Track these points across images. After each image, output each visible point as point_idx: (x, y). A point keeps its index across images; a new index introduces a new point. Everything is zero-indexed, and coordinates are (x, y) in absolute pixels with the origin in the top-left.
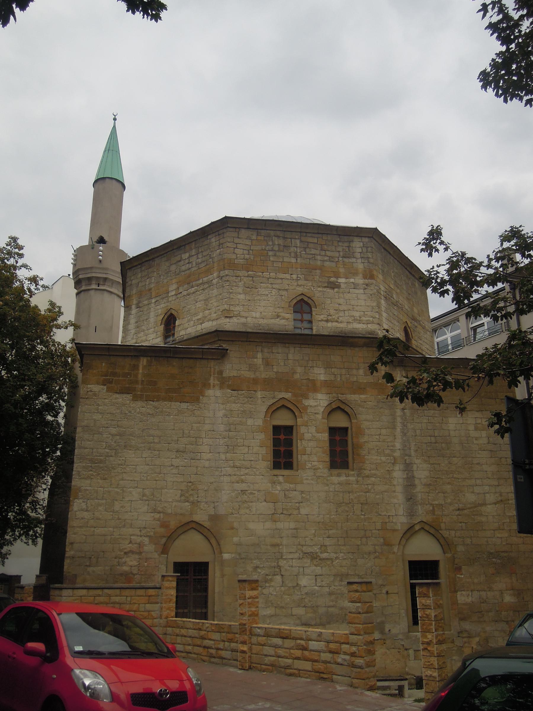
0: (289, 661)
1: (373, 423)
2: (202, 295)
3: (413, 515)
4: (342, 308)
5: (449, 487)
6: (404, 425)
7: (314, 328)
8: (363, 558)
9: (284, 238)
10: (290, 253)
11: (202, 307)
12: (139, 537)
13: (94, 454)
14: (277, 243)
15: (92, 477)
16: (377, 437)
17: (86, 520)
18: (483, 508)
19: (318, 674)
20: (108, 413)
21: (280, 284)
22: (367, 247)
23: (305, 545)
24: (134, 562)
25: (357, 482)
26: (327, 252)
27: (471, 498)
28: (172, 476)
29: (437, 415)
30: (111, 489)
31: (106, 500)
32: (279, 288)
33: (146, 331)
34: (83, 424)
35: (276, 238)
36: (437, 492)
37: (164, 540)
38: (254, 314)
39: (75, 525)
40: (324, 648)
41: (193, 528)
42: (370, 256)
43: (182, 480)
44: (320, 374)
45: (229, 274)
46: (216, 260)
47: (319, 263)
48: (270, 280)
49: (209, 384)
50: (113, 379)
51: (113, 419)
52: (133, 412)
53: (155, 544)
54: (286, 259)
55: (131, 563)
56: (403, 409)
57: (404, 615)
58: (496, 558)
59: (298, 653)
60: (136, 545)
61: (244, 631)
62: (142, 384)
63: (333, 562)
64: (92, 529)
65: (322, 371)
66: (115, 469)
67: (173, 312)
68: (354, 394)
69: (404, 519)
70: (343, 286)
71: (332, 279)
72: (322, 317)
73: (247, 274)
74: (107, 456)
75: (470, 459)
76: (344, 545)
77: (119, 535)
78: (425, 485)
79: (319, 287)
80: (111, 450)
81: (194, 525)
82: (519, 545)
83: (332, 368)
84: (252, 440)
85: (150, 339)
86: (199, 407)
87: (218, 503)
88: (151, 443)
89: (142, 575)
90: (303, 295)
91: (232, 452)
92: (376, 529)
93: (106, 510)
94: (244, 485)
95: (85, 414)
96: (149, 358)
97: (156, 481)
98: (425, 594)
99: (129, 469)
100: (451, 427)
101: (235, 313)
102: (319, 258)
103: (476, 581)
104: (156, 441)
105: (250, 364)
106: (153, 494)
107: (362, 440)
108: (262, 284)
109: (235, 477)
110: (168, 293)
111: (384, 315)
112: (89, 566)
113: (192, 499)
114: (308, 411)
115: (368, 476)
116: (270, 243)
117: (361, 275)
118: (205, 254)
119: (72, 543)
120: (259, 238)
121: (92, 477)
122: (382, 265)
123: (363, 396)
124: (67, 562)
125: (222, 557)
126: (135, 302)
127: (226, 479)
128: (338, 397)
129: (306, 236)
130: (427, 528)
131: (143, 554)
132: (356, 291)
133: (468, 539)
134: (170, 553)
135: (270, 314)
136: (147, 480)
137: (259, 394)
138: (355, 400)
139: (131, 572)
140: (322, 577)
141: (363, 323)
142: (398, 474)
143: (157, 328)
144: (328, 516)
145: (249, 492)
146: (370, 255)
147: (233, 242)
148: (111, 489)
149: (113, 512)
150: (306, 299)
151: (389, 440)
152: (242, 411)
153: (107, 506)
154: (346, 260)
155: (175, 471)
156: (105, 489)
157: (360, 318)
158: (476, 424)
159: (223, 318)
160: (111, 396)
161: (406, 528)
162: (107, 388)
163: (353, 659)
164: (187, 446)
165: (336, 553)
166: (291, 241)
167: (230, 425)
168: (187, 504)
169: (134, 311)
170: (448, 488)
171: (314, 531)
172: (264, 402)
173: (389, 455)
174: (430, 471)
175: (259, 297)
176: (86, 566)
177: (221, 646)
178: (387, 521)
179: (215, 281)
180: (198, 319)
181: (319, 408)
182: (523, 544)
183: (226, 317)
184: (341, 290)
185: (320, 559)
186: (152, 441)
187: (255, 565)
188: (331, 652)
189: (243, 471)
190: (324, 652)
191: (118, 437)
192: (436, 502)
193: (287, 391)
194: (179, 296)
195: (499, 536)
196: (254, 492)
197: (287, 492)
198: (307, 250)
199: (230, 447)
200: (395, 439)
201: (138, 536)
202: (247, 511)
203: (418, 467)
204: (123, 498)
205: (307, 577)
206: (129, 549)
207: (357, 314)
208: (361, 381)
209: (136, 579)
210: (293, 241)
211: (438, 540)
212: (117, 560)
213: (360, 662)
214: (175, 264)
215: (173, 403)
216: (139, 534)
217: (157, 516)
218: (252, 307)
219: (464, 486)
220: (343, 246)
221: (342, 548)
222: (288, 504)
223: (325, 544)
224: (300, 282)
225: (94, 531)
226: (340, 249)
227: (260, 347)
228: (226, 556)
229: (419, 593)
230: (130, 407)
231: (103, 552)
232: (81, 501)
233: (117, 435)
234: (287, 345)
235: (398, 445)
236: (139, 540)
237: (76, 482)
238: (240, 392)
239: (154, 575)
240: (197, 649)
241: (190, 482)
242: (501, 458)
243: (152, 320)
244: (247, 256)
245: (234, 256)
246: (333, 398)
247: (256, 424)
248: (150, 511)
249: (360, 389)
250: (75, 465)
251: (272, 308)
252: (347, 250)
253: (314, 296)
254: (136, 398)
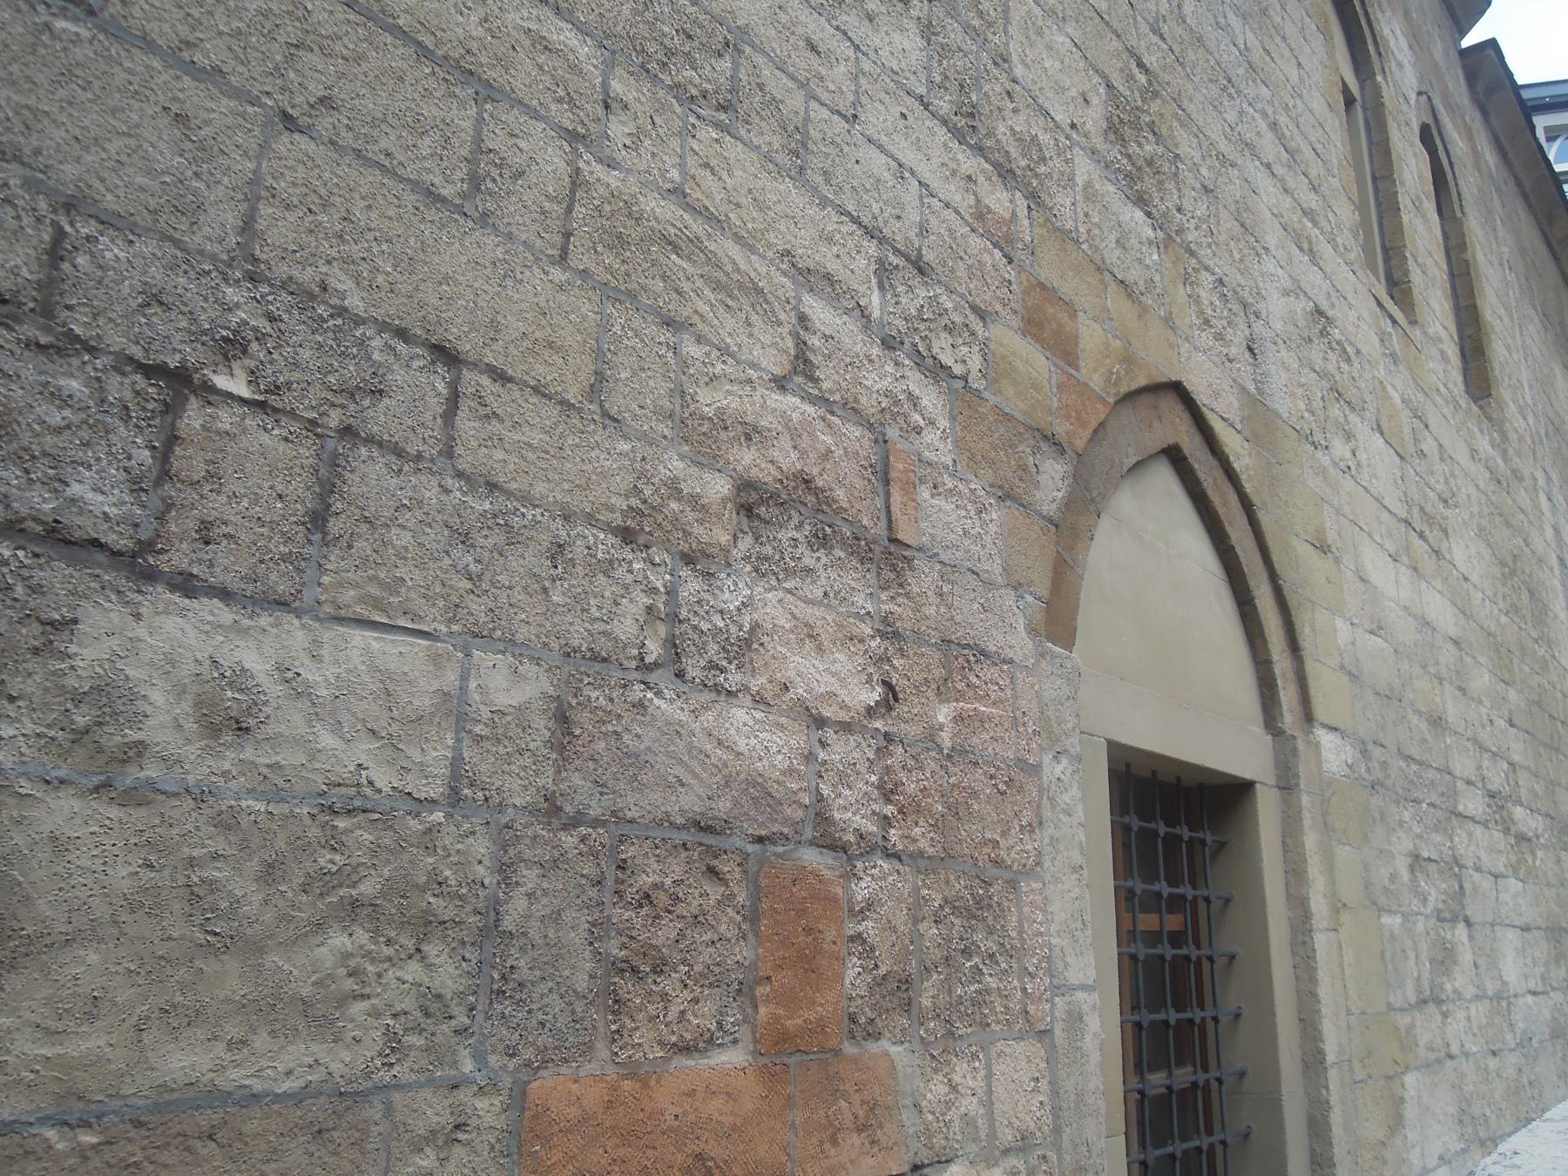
24: (843, 661)
77: (677, 192)
139: (822, 818)
206: (789, 460)
209: (868, 927)
231: (445, 355)
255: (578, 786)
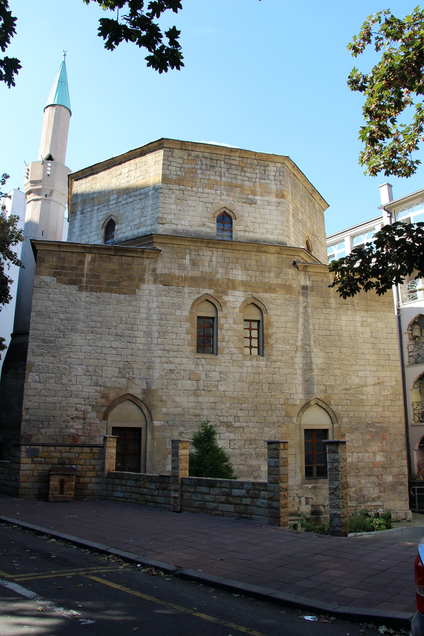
0: (215, 505)
1: (281, 317)
2: (139, 204)
3: (310, 393)
4: (257, 220)
5: (339, 371)
6: (306, 321)
7: (234, 236)
8: (268, 426)
9: (211, 159)
10: (215, 172)
11: (139, 215)
12: (84, 406)
13: (46, 335)
14: (204, 163)
15: (44, 354)
16: (284, 329)
17: (39, 390)
18: (365, 389)
19: (240, 514)
20: (57, 301)
21: (206, 198)
22: (280, 172)
23: (222, 416)
25: (266, 365)
26: (246, 173)
27: (355, 380)
28: (111, 356)
29: (332, 313)
30: (59, 365)
31: (56, 374)
32: (206, 201)
33: (89, 234)
34: (36, 309)
35: (204, 159)
36: (329, 375)
37: (104, 409)
38: (183, 222)
39: (29, 394)
40: (245, 494)
41: (128, 400)
42: (282, 179)
43: (120, 359)
44: (238, 275)
45: (164, 187)
46: (152, 174)
47: (239, 182)
48: (197, 193)
49: (144, 280)
50: (62, 272)
51: (62, 306)
52: (78, 300)
53: (97, 412)
54: (212, 177)
55: (76, 427)
56: (305, 307)
57: (299, 471)
58: (371, 428)
59: (223, 498)
60: (81, 412)
61: (176, 481)
62: (87, 277)
63: (244, 429)
64: (44, 398)
65: (240, 272)
66: (63, 348)
67: (113, 218)
68: (266, 292)
69: (301, 396)
70: (259, 202)
71: (251, 197)
72: (241, 228)
73: (178, 188)
74: (57, 337)
75: (356, 350)
76: (254, 416)
78: (320, 369)
79: (239, 202)
80: (60, 332)
81: (130, 397)
82: (390, 418)
83: (248, 270)
84: (180, 328)
85: (92, 240)
86: (136, 299)
87: (150, 380)
88: (94, 327)
89: (86, 436)
90: (225, 209)
91: (163, 338)
92: (279, 404)
93: (55, 382)
94: (172, 365)
95: (38, 301)
96: (93, 255)
97: (98, 359)
98: (334, 451)
99: (74, 349)
100: (343, 323)
101: (167, 220)
102: (239, 177)
103: (355, 445)
104: (98, 326)
105: (179, 264)
106: (95, 371)
107: (271, 331)
108: (191, 197)
109: (165, 359)
110: (109, 202)
111: (292, 229)
112: (42, 428)
113: (128, 376)
114: (227, 306)
115: (275, 361)
116: (199, 163)
117: (274, 194)
118: (142, 169)
119: (27, 409)
120: (190, 158)
121: (44, 354)
122: (291, 188)
123: (273, 295)
124: (23, 424)
125: (153, 423)
126: (80, 209)
127: (158, 360)
128: (253, 295)
129: (229, 159)
130: (320, 403)
131: (87, 420)
132: (270, 208)
133: (351, 413)
134: (109, 420)
135: (197, 222)
136: (90, 359)
137: (186, 290)
138: (267, 298)
139: (77, 434)
140: (235, 441)
141: (274, 235)
142: (299, 360)
143: (98, 231)
144: (241, 393)
145: (176, 371)
146: (282, 178)
147: (168, 160)
148: (59, 365)
149: (62, 384)
150: (228, 212)
151: (293, 332)
152: (172, 303)
153: (56, 379)
154: (262, 181)
155: (114, 352)
156: (55, 365)
157: (272, 230)
158: (362, 321)
159: (157, 224)
160: (60, 286)
161: (303, 403)
162: (57, 279)
163: (270, 502)
164: (124, 331)
165: (247, 422)
166: (217, 162)
167: (161, 314)
168: (123, 379)
169: (79, 216)
170: (338, 372)
171: (229, 405)
172: (190, 296)
173: (293, 345)
174: (325, 358)
175: (188, 208)
176: (39, 428)
177: (156, 493)
178: (289, 397)
179: (150, 193)
180: (135, 225)
181: (237, 303)
182: (393, 416)
183: (159, 223)
184: (257, 206)
185: (234, 427)
186: (95, 326)
187: (180, 431)
188: (251, 497)
189: (172, 354)
190: (246, 497)
191: (66, 322)
192: (328, 384)
193: (210, 288)
194: (119, 204)
195: (375, 410)
196: (180, 371)
197: (207, 372)
198: (230, 171)
199: (161, 334)
200: (298, 331)
201: (82, 404)
202: (175, 387)
203: (315, 355)
204: (70, 373)
205: (223, 441)
207: (270, 227)
208: (272, 282)
210: (218, 162)
211: (328, 413)
212: (65, 424)
213: (276, 505)
214: (116, 177)
215: (113, 294)
216: (83, 403)
217: (98, 389)
218: (182, 216)
219: (350, 370)
220: (260, 169)
221: (251, 418)
222: (208, 382)
223: (238, 415)
224: (223, 197)
225: (46, 399)
226: (257, 171)
227: (189, 250)
228: (156, 423)
229: (329, 450)
230: (76, 296)
231: (54, 417)
232: (34, 374)
233: (65, 320)
234: (211, 249)
235: (300, 337)
236: (83, 408)
237: (30, 358)
238: (170, 287)
239: (96, 437)
240: (134, 496)
241: (127, 362)
242: (380, 349)
243: (94, 225)
244: (179, 173)
245: (168, 172)
246: (248, 295)
247: (183, 314)
248: (92, 384)
249: (270, 289)
250: (30, 344)
251: (198, 219)
252: (263, 173)
253: (235, 210)
254: (81, 289)
255: (61, 434)
